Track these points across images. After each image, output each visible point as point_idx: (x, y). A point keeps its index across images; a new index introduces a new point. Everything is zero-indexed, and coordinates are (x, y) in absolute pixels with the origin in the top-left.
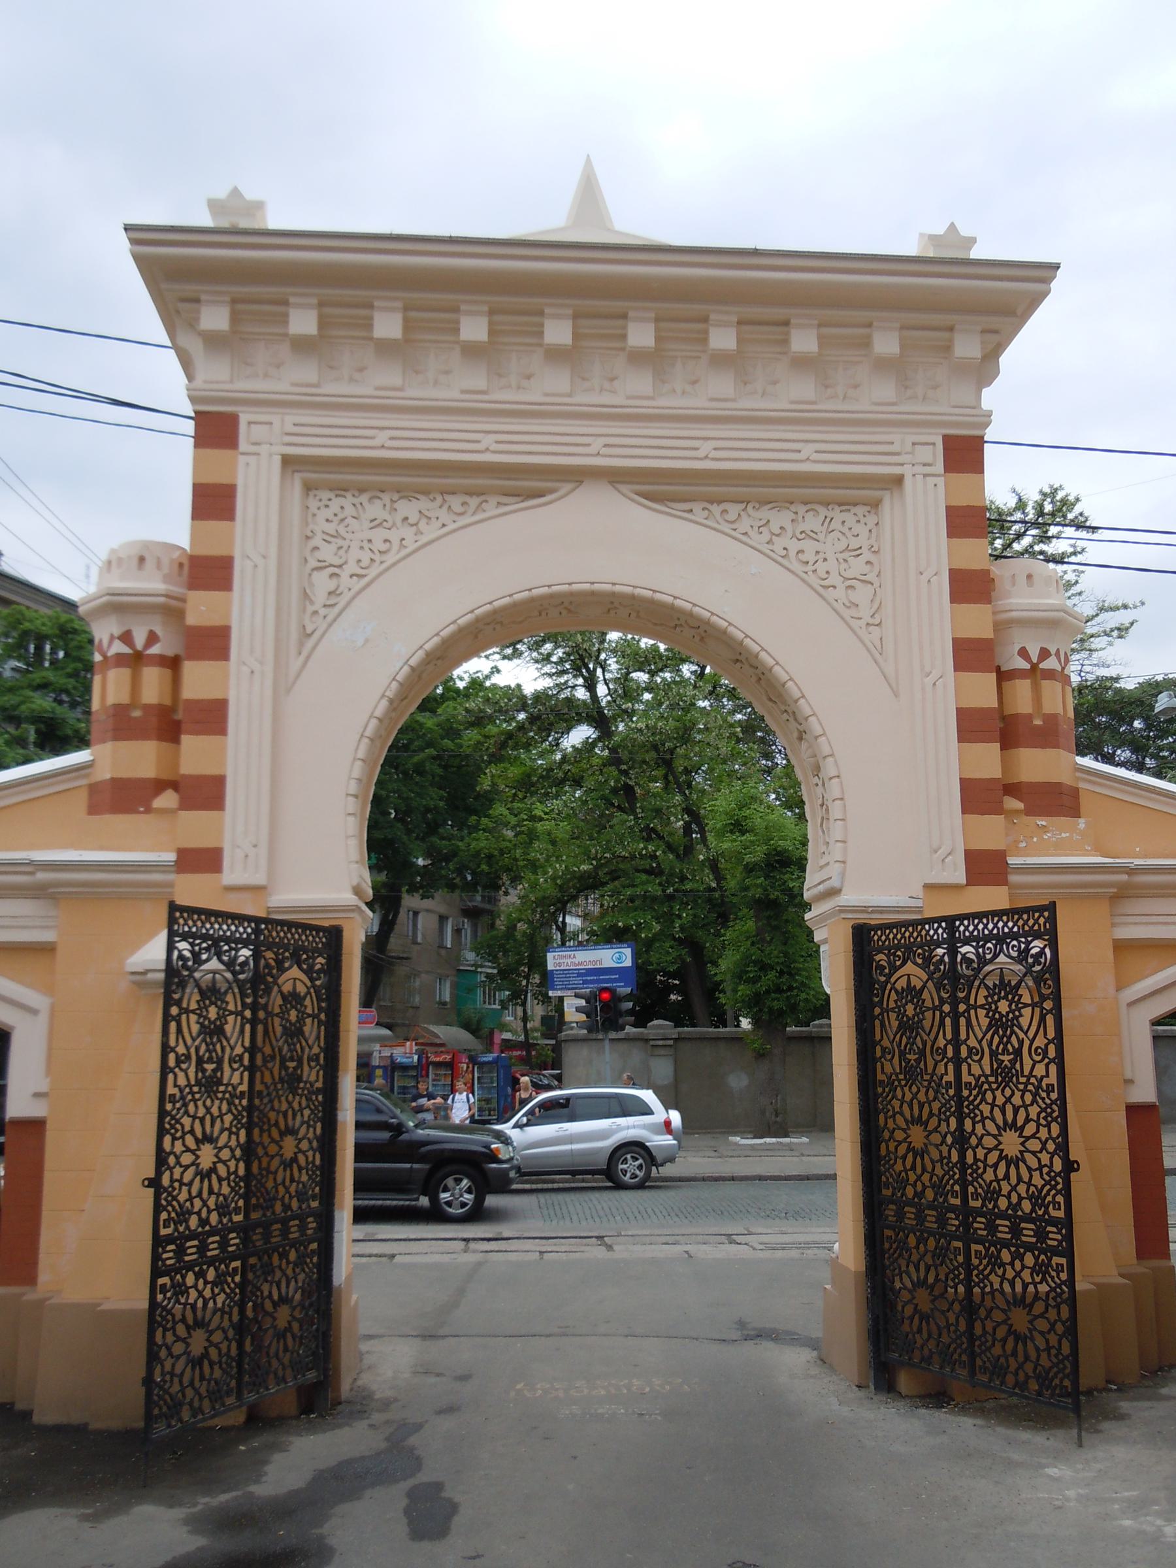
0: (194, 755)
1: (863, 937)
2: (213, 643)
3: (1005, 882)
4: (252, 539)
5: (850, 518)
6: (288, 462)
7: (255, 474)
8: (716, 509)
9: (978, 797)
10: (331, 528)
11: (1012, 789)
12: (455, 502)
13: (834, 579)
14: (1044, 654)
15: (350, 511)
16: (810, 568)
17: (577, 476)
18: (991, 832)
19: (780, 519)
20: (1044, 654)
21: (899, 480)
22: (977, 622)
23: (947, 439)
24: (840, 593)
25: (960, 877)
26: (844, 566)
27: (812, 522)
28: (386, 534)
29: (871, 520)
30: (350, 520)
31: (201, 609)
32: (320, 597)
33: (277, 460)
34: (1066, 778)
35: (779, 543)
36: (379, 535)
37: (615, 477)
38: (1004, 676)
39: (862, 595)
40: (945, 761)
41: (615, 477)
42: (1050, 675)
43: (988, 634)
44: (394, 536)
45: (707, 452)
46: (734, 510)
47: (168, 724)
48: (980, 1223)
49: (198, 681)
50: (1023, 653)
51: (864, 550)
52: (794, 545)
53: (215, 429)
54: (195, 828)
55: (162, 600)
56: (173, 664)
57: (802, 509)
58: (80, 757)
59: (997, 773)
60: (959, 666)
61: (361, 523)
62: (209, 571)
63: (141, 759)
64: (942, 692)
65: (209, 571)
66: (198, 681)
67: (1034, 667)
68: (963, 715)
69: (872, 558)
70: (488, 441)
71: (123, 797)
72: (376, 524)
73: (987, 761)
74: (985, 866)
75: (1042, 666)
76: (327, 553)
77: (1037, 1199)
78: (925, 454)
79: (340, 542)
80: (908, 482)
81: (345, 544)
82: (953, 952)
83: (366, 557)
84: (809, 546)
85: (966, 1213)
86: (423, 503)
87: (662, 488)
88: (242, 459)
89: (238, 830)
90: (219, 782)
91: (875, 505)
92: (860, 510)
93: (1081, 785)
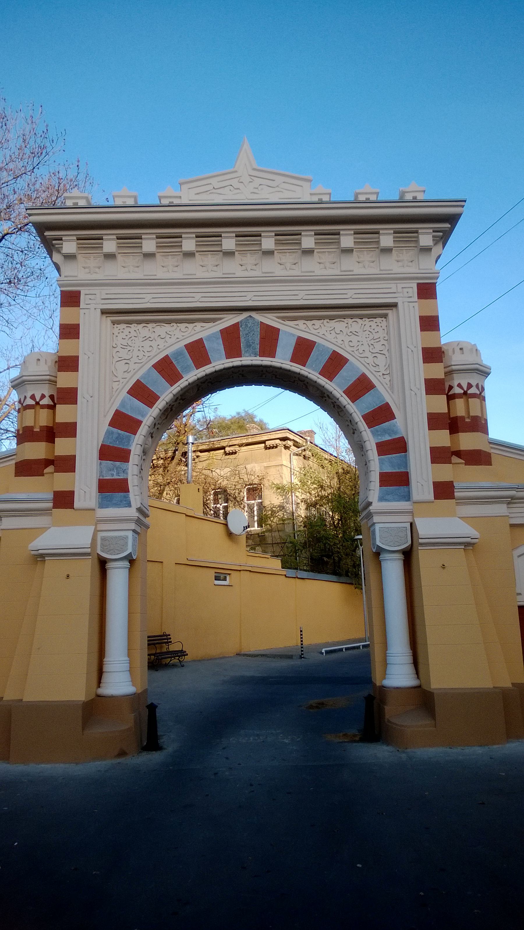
2: (69, 396)
3: (453, 497)
4: (84, 347)
5: (373, 324)
6: (104, 312)
7: (88, 317)
8: (309, 323)
10: (124, 342)
11: (458, 454)
13: (367, 354)
14: (470, 386)
15: (133, 334)
16: (355, 349)
18: (446, 472)
20: (470, 386)
22: (437, 371)
23: (419, 285)
24: (370, 360)
25: (431, 497)
26: (372, 347)
28: (151, 343)
29: (384, 324)
30: (133, 338)
31: (65, 380)
33: (99, 311)
35: (340, 337)
36: (148, 343)
38: (451, 398)
42: (474, 396)
43: (442, 376)
44: (154, 344)
46: (317, 323)
50: (459, 386)
51: (381, 339)
52: (347, 339)
53: (70, 299)
54: (61, 481)
55: (48, 377)
56: (52, 407)
57: (350, 321)
59: (449, 445)
60: (428, 392)
62: (68, 363)
65: (68, 363)
67: (465, 393)
69: (385, 343)
72: (146, 339)
73: (443, 438)
75: (469, 392)
76: (124, 354)
79: (129, 348)
80: (400, 305)
81: (132, 348)
83: (141, 354)
84: (354, 338)
88: (82, 312)
92: (378, 320)
93: (492, 451)
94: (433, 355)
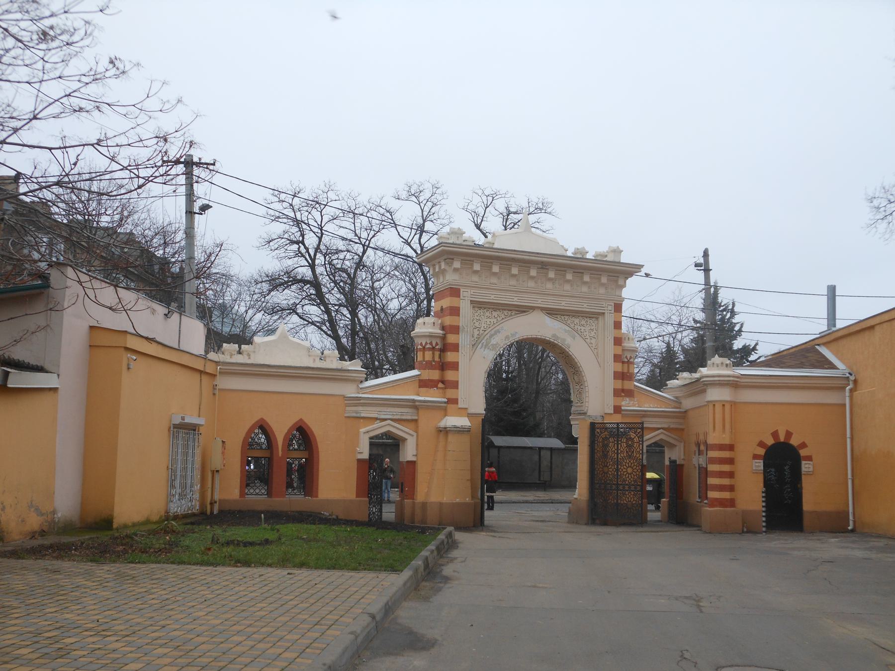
0: (450, 375)
1: (593, 426)
2: (455, 348)
9: (617, 393)
11: (623, 390)
12: (505, 312)
14: (631, 358)
17: (533, 308)
19: (577, 321)
20: (631, 358)
21: (604, 313)
22: (619, 351)
27: (583, 322)
32: (476, 336)
34: (632, 388)
36: (488, 320)
37: (542, 309)
39: (593, 341)
40: (611, 384)
41: (542, 309)
44: (492, 320)
45: (563, 304)
46: (567, 317)
47: (443, 366)
48: (621, 487)
49: (450, 357)
54: (450, 393)
58: (415, 372)
61: (487, 319)
63: (435, 375)
64: (611, 367)
66: (450, 357)
68: (615, 373)
70: (516, 299)
71: (424, 384)
73: (619, 384)
74: (617, 409)
76: (477, 324)
77: (635, 481)
78: (610, 308)
82: (618, 430)
84: (582, 328)
85: (618, 484)
86: (498, 313)
87: (552, 312)
89: (461, 393)
90: (457, 382)
91: (597, 318)
94: (618, 341)
